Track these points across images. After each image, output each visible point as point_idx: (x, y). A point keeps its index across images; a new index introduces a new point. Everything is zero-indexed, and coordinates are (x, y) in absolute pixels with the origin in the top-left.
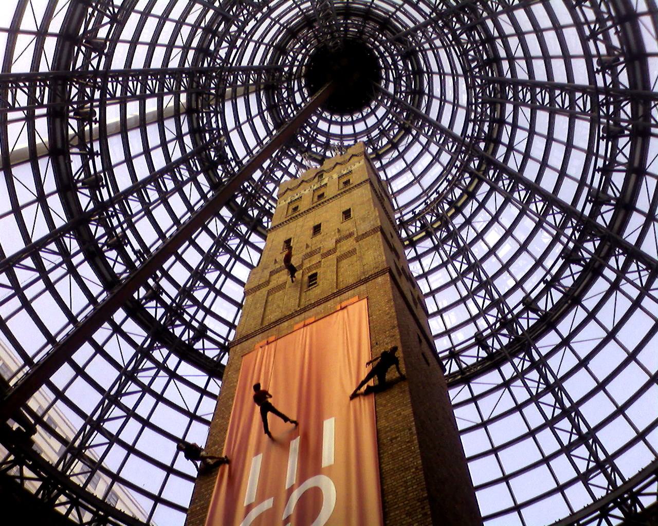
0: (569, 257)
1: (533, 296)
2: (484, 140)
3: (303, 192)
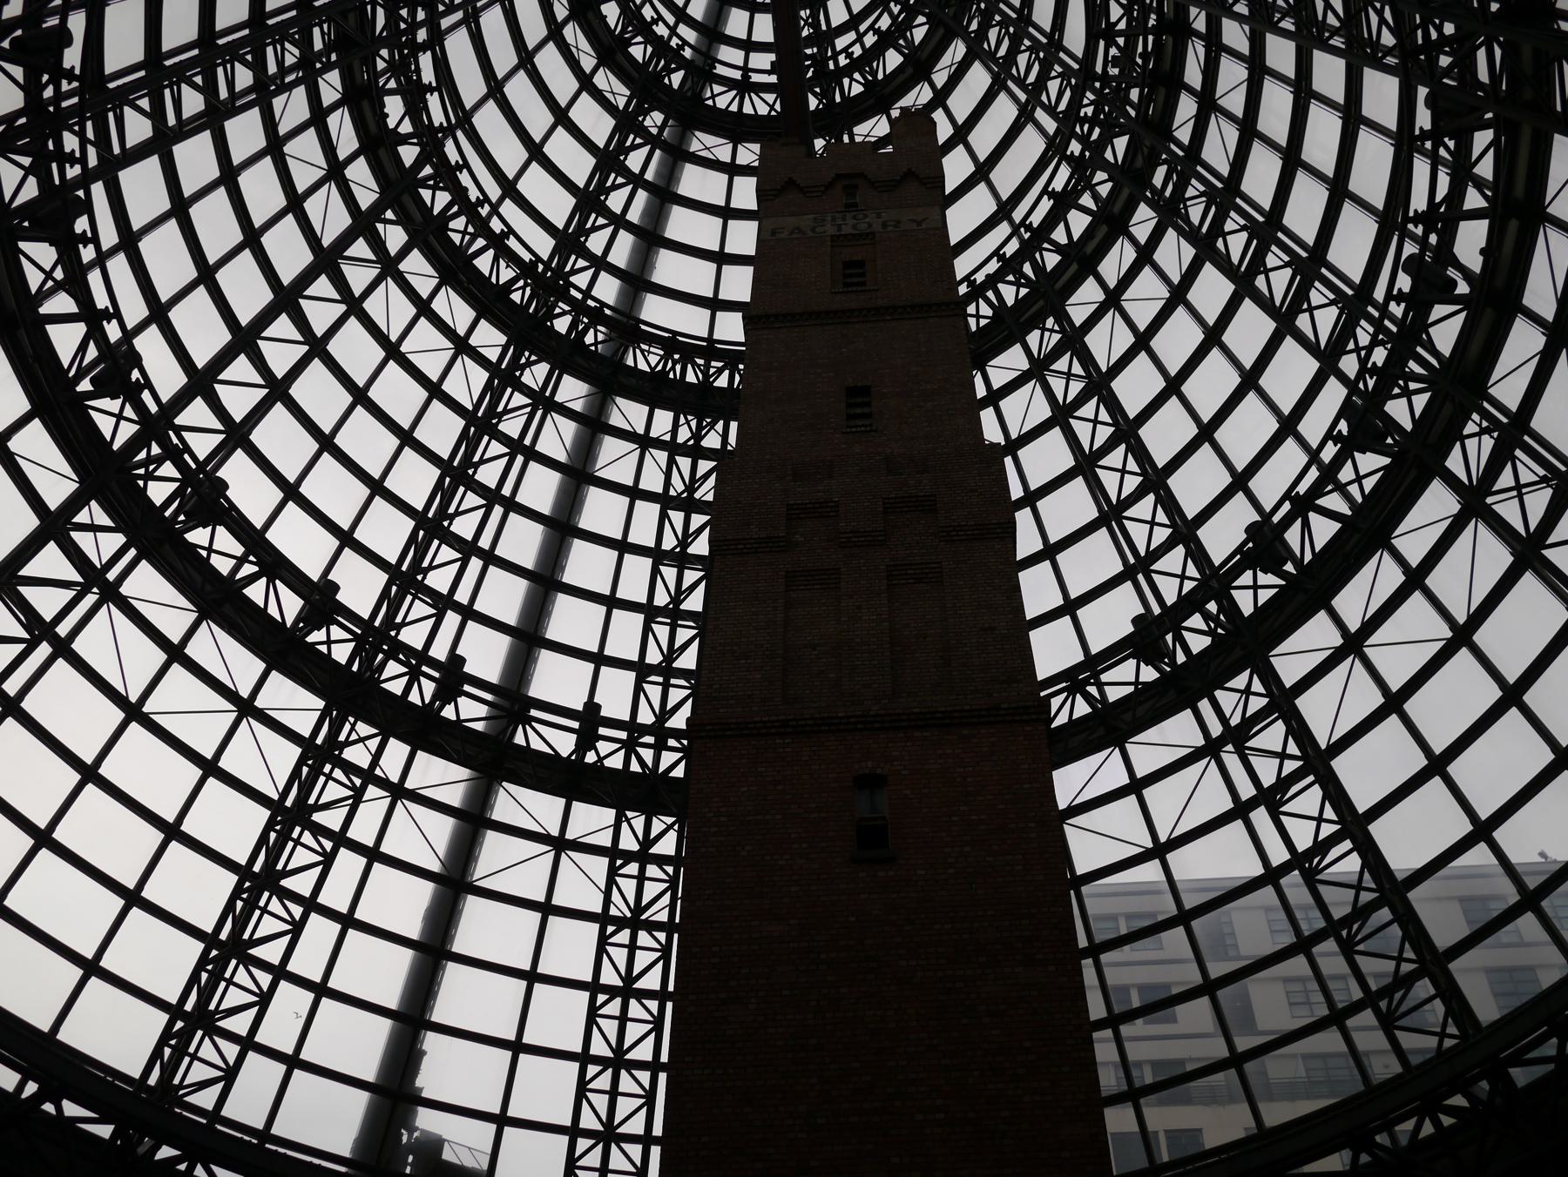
1: (1276, 519)
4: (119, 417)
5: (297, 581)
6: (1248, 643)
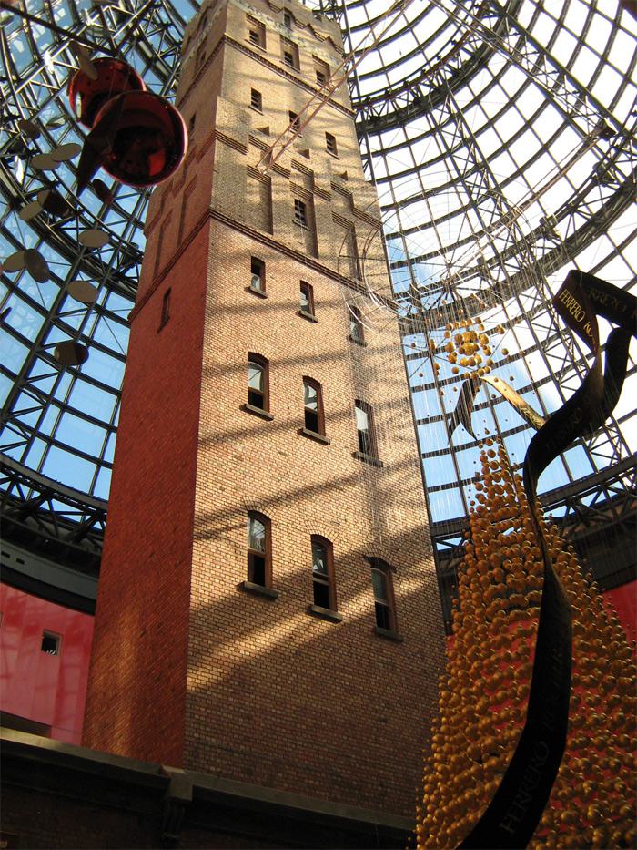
0: (601, 176)
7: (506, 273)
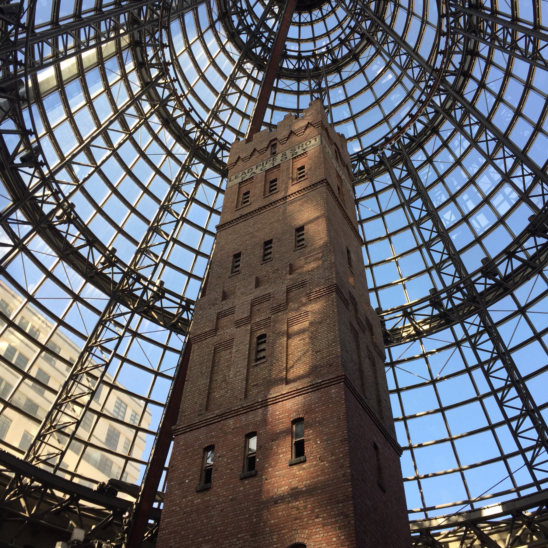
2: (452, 74)
3: (254, 170)
4: (33, 176)
5: (102, 248)
6: (478, 304)
7: (452, 303)
